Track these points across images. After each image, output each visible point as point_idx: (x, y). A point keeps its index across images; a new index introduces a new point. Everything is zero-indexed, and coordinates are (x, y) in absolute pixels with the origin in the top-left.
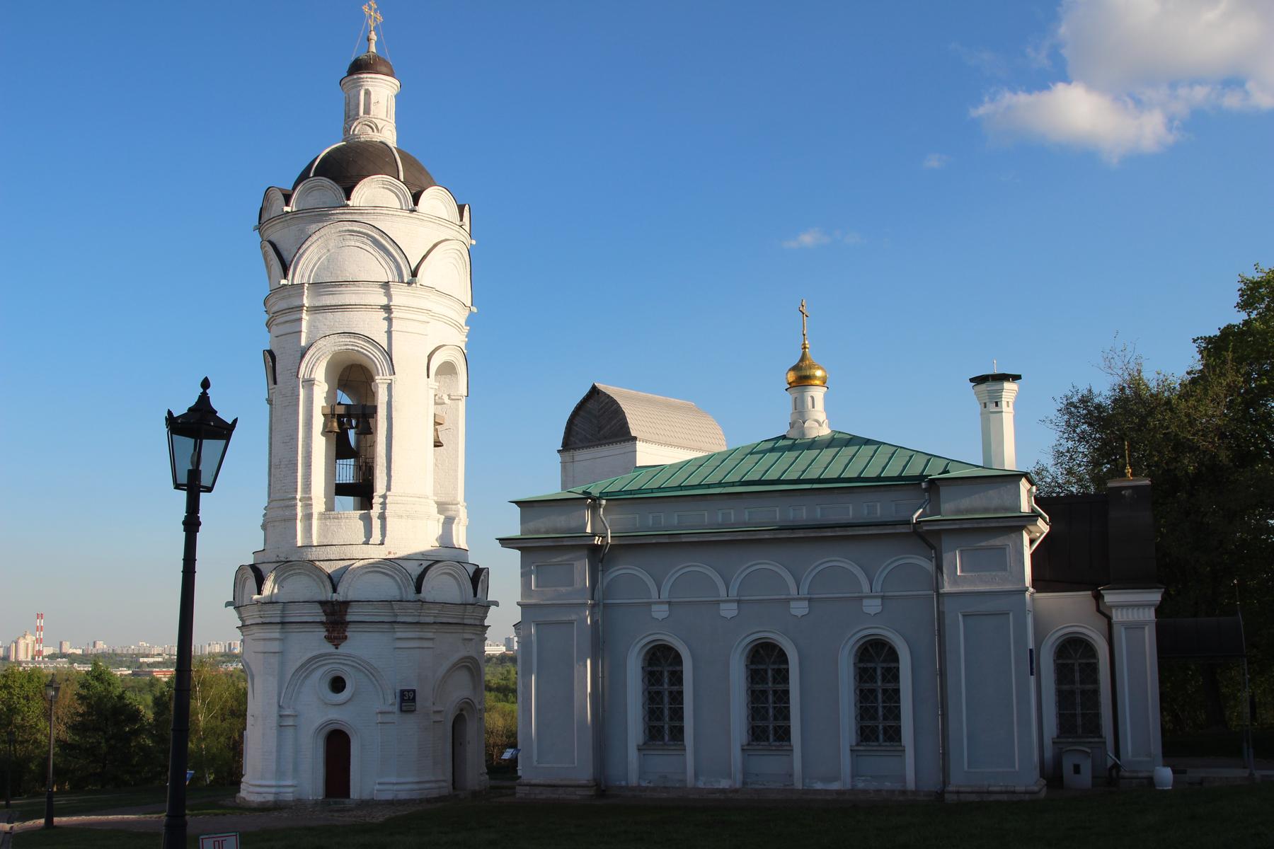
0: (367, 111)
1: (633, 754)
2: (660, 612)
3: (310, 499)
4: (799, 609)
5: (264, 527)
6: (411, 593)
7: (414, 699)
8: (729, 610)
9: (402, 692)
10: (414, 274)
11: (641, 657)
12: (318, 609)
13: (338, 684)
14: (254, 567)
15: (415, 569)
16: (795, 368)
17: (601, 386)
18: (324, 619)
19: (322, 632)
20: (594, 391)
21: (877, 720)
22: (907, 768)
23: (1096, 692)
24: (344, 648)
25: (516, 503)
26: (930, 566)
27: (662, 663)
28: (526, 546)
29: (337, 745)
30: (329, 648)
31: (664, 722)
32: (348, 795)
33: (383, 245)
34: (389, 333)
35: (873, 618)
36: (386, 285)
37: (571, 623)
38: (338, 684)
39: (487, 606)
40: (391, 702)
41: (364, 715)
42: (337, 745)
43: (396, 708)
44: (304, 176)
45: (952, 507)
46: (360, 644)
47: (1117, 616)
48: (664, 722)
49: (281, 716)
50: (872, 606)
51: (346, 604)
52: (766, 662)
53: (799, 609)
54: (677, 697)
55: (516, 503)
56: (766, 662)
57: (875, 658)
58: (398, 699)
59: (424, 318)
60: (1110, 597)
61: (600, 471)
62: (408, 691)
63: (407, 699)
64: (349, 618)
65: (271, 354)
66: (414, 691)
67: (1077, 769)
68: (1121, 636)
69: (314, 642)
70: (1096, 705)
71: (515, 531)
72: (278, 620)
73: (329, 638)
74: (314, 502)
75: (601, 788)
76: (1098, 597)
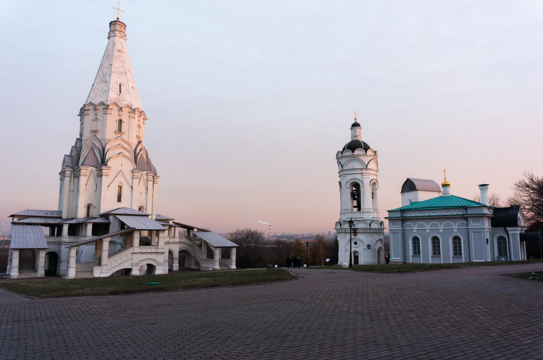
4: (441, 231)
5: (340, 214)
6: (369, 227)
14: (339, 222)
15: (369, 222)
20: (408, 180)
21: (457, 251)
23: (506, 247)
24: (357, 237)
26: (466, 223)
27: (416, 240)
28: (390, 219)
31: (417, 251)
33: (361, 162)
36: (361, 169)
39: (384, 229)
40: (365, 247)
41: (361, 249)
44: (344, 149)
45: (470, 211)
46: (359, 236)
47: (509, 232)
48: (417, 251)
52: (435, 240)
53: (441, 231)
54: (419, 246)
56: (435, 240)
57: (456, 239)
60: (508, 229)
61: (411, 196)
63: (369, 246)
65: (340, 183)
68: (511, 236)
70: (506, 250)
71: (387, 216)
76: (505, 229)
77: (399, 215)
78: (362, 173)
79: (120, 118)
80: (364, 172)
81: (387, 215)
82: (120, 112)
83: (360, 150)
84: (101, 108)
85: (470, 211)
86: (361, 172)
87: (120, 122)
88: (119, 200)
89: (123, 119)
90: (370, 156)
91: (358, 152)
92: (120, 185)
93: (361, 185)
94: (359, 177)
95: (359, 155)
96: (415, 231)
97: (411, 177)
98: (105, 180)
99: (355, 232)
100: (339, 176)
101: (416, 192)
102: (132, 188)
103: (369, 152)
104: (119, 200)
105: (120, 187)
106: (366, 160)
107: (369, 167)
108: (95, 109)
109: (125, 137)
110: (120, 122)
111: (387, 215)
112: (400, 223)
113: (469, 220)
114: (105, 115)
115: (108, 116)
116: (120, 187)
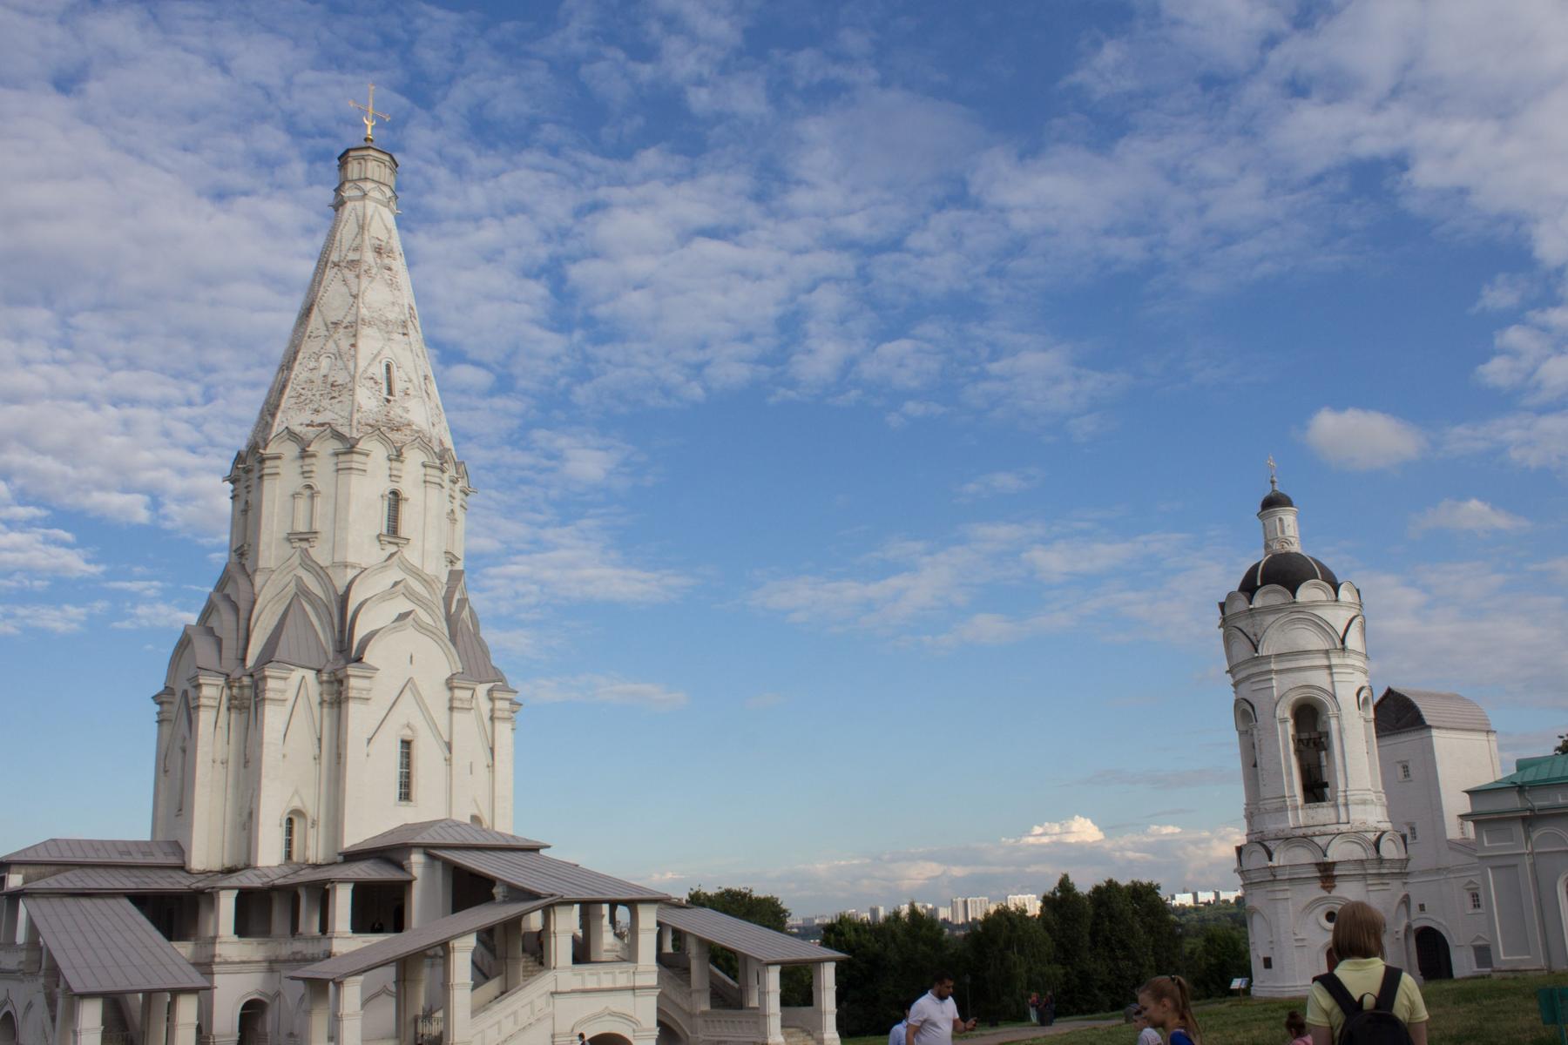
0: (1283, 532)
6: (1372, 854)
10: (1343, 641)
12: (1314, 869)
15: (1372, 837)
17: (1394, 687)
19: (1318, 884)
20: (1390, 692)
24: (1335, 893)
33: (1323, 627)
36: (1327, 652)
37: (1515, 866)
51: (1334, 863)
69: (1315, 891)
71: (1467, 809)
73: (1324, 888)
75: (1551, 972)
77: (1513, 802)
79: (395, 486)
81: (1465, 805)
82: (395, 464)
83: (1316, 586)
84: (324, 449)
86: (1325, 662)
87: (396, 498)
88: (405, 794)
89: (406, 488)
90: (1349, 606)
91: (1308, 593)
92: (407, 734)
93: (1332, 710)
94: (1320, 679)
95: (1315, 604)
97: (1400, 688)
98: (359, 718)
99: (1327, 874)
100: (1235, 685)
101: (1424, 733)
102: (449, 746)
103: (1344, 594)
104: (405, 794)
105: (406, 744)
106: (1338, 618)
107: (1349, 643)
108: (304, 454)
109: (411, 555)
110: (396, 498)
111: (1465, 805)
114: (342, 476)
115: (355, 478)
116: (406, 744)
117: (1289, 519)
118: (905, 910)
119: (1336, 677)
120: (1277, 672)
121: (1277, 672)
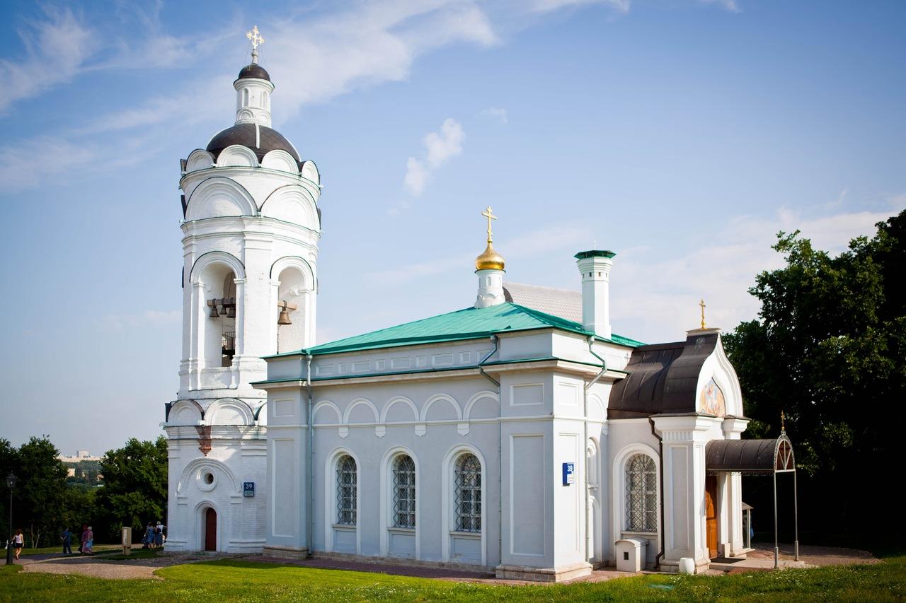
1: (329, 532)
2: (343, 432)
3: (197, 360)
6: (250, 421)
7: (253, 489)
8: (380, 432)
9: (245, 484)
11: (335, 463)
12: (195, 431)
13: (210, 478)
16: (480, 257)
18: (199, 437)
19: (197, 446)
22: (480, 550)
24: (209, 456)
25: (265, 358)
26: (497, 399)
29: (210, 515)
30: (201, 456)
32: (215, 549)
33: (241, 195)
34: (243, 250)
35: (466, 439)
38: (210, 478)
40: (238, 491)
41: (225, 499)
42: (210, 515)
43: (241, 495)
46: (220, 454)
49: (179, 498)
50: (463, 429)
53: (420, 431)
55: (265, 358)
58: (243, 488)
59: (269, 239)
60: (662, 423)
62: (249, 483)
64: (211, 438)
66: (253, 484)
67: (626, 556)
71: (264, 378)
72: (176, 437)
74: (199, 363)
76: (652, 423)
78: (242, 234)
80: (248, 228)
85: (508, 349)
90: (279, 173)
94: (230, 246)
96: (343, 432)
112: (297, 399)
113: (503, 382)
117: (256, 89)
118: (55, 449)
119: (248, 244)
120: (197, 238)
121: (197, 238)
